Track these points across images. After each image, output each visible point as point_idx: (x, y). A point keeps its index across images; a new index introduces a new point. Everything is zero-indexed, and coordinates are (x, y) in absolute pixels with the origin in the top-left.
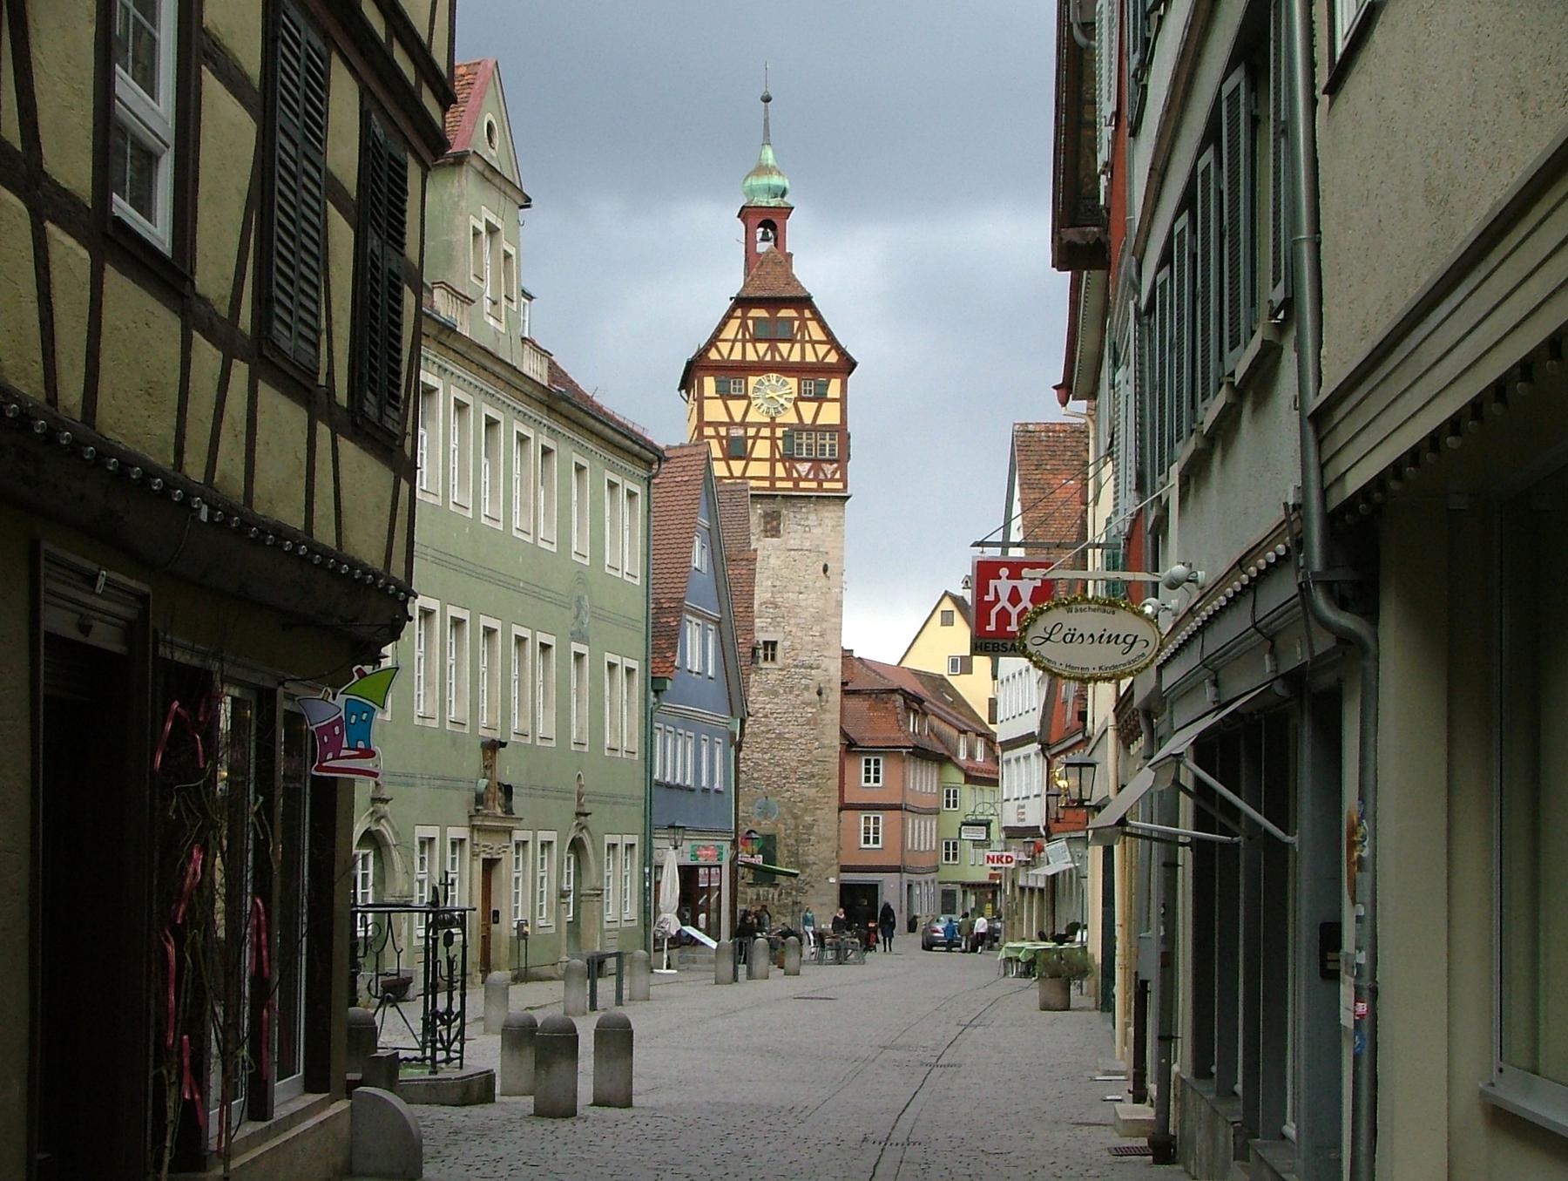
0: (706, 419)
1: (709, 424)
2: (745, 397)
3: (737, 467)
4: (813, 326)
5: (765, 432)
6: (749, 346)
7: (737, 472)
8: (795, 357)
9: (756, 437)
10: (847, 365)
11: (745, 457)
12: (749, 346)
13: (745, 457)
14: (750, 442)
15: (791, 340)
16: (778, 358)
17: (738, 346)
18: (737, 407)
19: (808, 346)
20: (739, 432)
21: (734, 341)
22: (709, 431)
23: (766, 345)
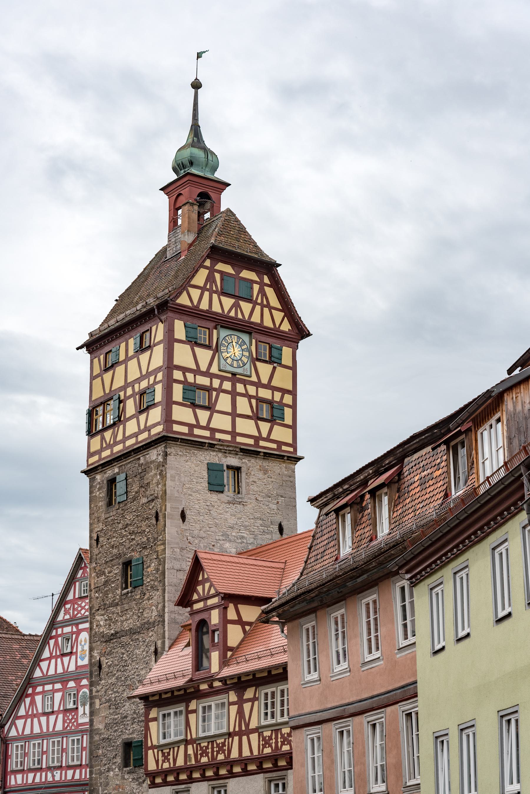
0: (176, 362)
1: (178, 368)
2: (208, 347)
3: (203, 415)
4: (270, 292)
5: (227, 386)
6: (215, 296)
7: (203, 423)
8: (256, 318)
9: (220, 390)
10: (301, 332)
11: (210, 408)
12: (215, 296)
13: (210, 408)
14: (214, 393)
15: (249, 300)
16: (240, 316)
17: (207, 294)
18: (204, 356)
19: (266, 310)
20: (203, 381)
21: (203, 289)
22: (178, 375)
23: (231, 301)
